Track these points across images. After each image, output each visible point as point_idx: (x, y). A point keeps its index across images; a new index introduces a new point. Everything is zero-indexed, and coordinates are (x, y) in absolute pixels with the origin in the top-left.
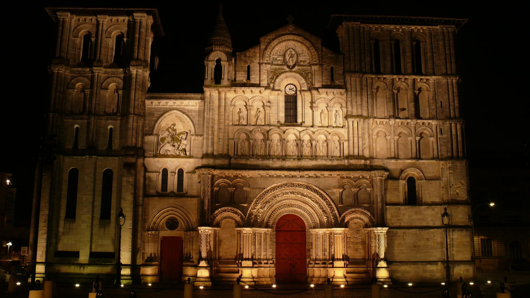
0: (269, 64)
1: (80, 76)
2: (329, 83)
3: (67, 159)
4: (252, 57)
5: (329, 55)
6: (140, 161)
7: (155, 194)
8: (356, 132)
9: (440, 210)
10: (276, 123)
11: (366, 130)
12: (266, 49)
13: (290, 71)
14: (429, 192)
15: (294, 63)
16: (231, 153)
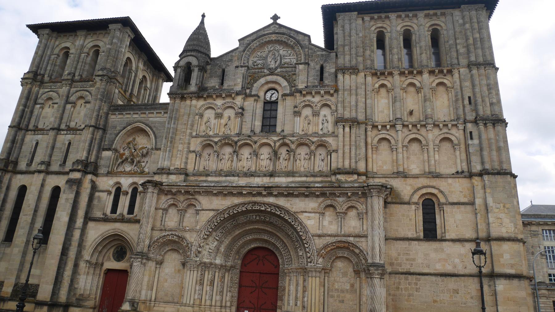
0: (245, 66)
1: (51, 91)
2: (317, 84)
3: (19, 176)
4: (228, 61)
5: (318, 53)
6: (89, 177)
7: (102, 216)
8: (347, 139)
9: (472, 246)
10: (249, 132)
11: (363, 137)
12: (244, 51)
13: (272, 73)
14: (454, 222)
15: (276, 65)
16: (190, 168)
